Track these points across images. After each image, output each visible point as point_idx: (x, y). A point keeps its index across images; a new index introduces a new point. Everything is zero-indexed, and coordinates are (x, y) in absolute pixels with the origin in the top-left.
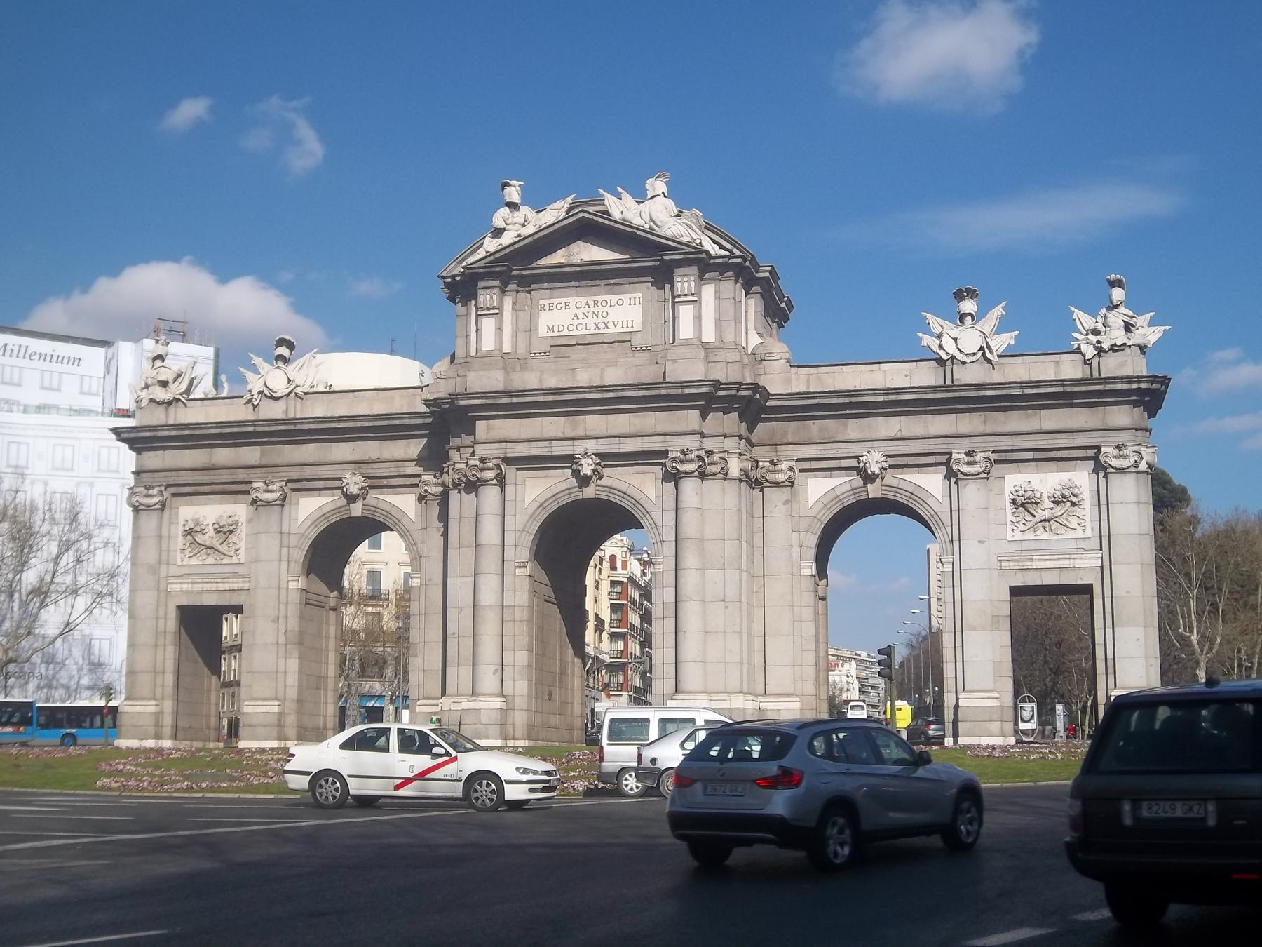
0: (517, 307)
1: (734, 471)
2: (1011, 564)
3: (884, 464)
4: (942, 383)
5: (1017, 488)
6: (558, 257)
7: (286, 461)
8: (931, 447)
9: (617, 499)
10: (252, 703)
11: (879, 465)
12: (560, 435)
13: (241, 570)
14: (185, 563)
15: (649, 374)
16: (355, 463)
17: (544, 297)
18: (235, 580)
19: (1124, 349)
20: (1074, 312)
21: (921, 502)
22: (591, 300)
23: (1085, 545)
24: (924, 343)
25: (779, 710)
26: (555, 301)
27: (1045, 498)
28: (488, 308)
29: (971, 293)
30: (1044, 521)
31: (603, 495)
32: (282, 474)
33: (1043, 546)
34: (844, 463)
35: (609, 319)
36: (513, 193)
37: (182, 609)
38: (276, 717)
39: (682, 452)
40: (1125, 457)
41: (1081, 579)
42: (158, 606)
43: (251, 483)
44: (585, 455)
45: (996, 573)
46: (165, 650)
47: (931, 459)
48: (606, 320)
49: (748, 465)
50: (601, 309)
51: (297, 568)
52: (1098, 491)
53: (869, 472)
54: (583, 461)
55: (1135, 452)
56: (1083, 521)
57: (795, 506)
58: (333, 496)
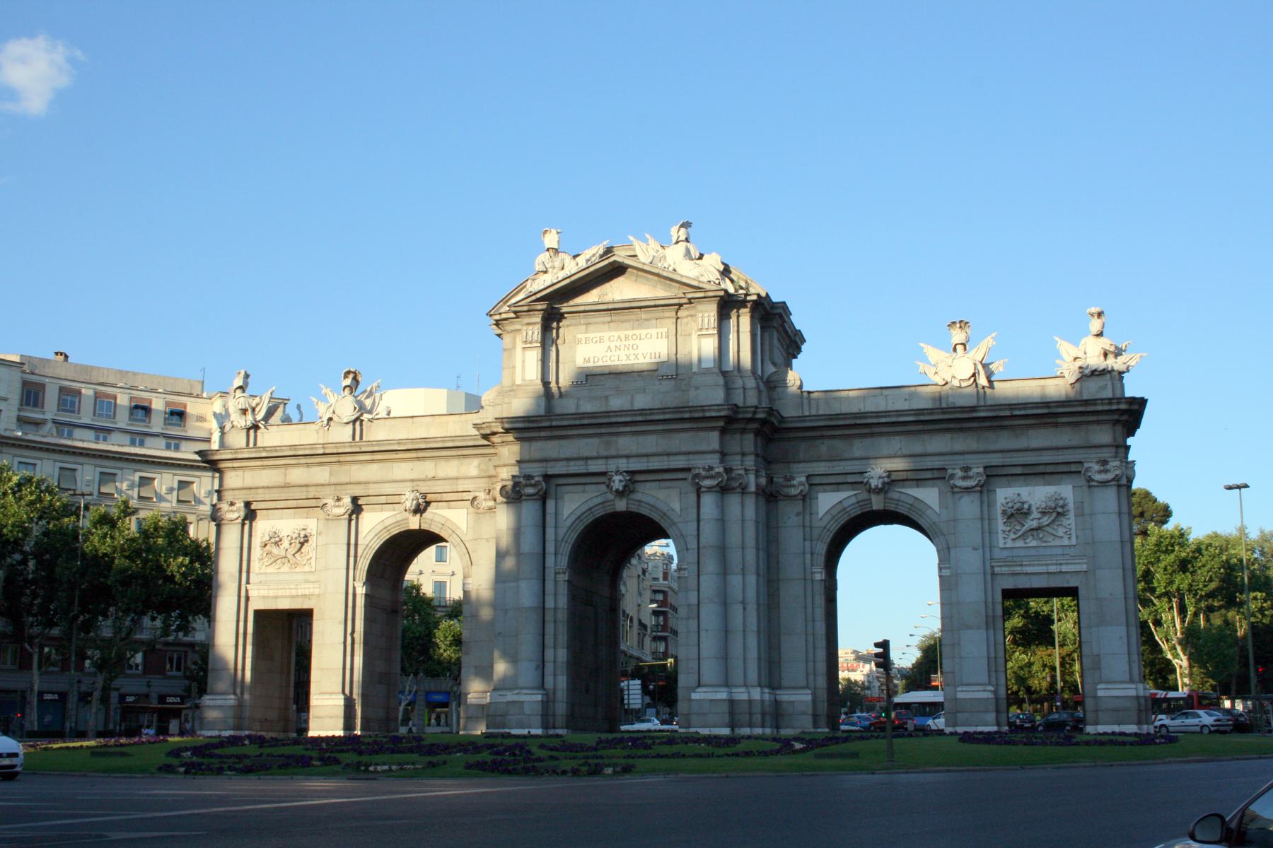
2: (1004, 569)
3: (886, 480)
4: (938, 406)
5: (1008, 500)
6: (592, 296)
7: (353, 480)
8: (929, 464)
9: (645, 511)
10: (321, 696)
11: (881, 480)
12: (594, 454)
13: (311, 577)
14: (262, 571)
15: (671, 401)
16: (412, 481)
18: (306, 586)
19: (1104, 374)
20: (1057, 342)
21: (921, 514)
22: (623, 334)
23: (1072, 551)
24: (921, 370)
25: (793, 702)
26: (590, 335)
27: (1034, 509)
28: (531, 343)
29: (963, 324)
30: (1033, 530)
31: (634, 508)
32: (348, 492)
33: (1033, 552)
34: (851, 479)
36: (551, 240)
37: (259, 614)
39: (704, 469)
40: (1106, 471)
41: (1068, 582)
44: (617, 472)
45: (989, 577)
47: (928, 475)
48: (636, 352)
49: (763, 481)
50: (631, 342)
52: (1082, 502)
53: (873, 486)
54: (617, 478)
55: (1114, 467)
57: (807, 518)
58: (394, 510)
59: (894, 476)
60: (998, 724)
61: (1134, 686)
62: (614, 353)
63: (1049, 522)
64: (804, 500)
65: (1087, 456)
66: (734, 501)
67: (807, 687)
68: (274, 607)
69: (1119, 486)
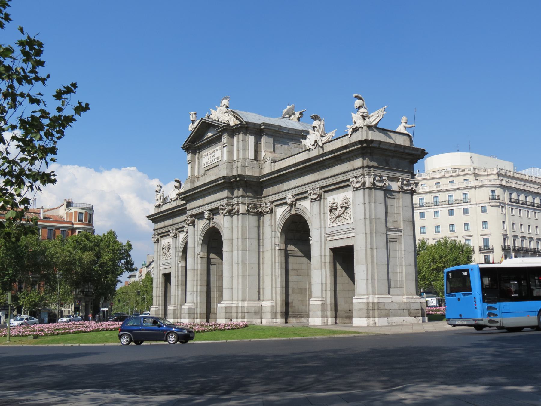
0: (200, 158)
1: (241, 212)
2: (330, 238)
3: (293, 199)
8: (304, 189)
17: (204, 153)
26: (205, 154)
27: (339, 206)
33: (339, 228)
34: (284, 201)
35: (215, 158)
38: (173, 311)
42: (157, 274)
43: (169, 231)
46: (159, 289)
51: (180, 259)
56: (350, 215)
59: (296, 198)
60: (324, 316)
61: (366, 297)
62: (210, 160)
63: (342, 211)
64: (272, 213)
65: (352, 175)
66: (235, 217)
67: (272, 300)
68: (165, 273)
69: (364, 189)
